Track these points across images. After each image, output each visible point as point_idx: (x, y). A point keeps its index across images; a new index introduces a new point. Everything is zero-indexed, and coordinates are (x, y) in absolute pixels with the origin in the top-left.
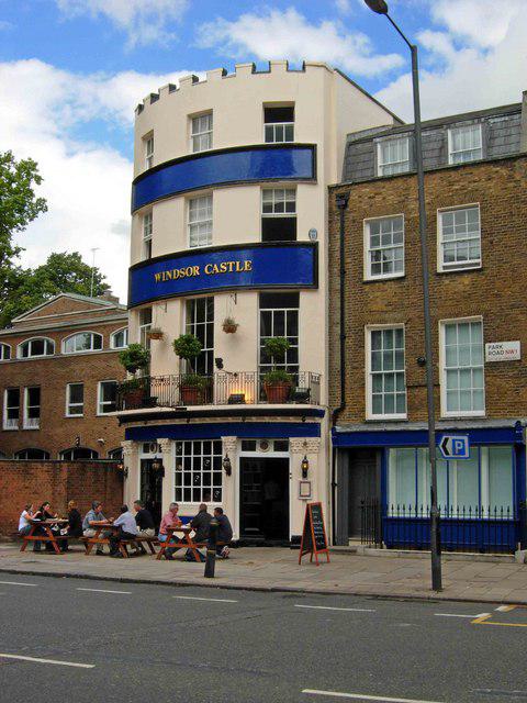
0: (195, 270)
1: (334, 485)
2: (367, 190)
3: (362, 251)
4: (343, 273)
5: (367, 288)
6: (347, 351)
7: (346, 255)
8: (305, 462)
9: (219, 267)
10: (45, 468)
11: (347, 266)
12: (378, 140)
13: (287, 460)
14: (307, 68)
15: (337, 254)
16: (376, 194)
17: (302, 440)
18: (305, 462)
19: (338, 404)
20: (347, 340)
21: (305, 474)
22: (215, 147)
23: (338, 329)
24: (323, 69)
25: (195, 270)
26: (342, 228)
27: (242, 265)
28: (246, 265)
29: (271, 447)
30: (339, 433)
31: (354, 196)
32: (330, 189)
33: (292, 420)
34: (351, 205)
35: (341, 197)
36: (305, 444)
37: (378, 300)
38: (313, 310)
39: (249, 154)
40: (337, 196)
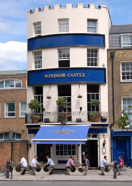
0: (64, 75)
1: (111, 149)
2: (121, 52)
3: (120, 72)
4: (113, 79)
5: (122, 84)
6: (115, 105)
7: (114, 73)
8: (105, 141)
9: (73, 75)
10: (9, 145)
11: (114, 77)
12: (122, 34)
13: (97, 141)
14: (101, 8)
15: (111, 72)
16: (125, 54)
17: (103, 134)
18: (105, 141)
19: (112, 122)
20: (114, 101)
21: (104, 145)
22: (70, 33)
23: (111, 97)
24: (106, 9)
25: (64, 75)
26: (112, 63)
27: (82, 75)
28: (83, 75)
29: (91, 137)
30: (115, 132)
31: (117, 53)
32: (108, 50)
33: (100, 127)
34: (115, 56)
35: (111, 53)
36: (104, 135)
37: (126, 89)
38: (104, 91)
39: (71, 36)
40: (110, 52)
